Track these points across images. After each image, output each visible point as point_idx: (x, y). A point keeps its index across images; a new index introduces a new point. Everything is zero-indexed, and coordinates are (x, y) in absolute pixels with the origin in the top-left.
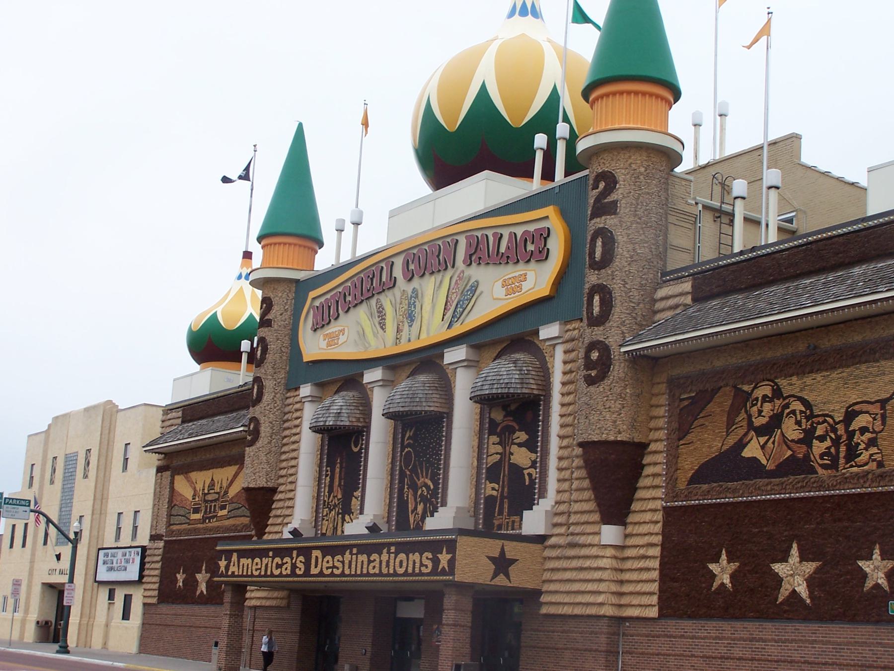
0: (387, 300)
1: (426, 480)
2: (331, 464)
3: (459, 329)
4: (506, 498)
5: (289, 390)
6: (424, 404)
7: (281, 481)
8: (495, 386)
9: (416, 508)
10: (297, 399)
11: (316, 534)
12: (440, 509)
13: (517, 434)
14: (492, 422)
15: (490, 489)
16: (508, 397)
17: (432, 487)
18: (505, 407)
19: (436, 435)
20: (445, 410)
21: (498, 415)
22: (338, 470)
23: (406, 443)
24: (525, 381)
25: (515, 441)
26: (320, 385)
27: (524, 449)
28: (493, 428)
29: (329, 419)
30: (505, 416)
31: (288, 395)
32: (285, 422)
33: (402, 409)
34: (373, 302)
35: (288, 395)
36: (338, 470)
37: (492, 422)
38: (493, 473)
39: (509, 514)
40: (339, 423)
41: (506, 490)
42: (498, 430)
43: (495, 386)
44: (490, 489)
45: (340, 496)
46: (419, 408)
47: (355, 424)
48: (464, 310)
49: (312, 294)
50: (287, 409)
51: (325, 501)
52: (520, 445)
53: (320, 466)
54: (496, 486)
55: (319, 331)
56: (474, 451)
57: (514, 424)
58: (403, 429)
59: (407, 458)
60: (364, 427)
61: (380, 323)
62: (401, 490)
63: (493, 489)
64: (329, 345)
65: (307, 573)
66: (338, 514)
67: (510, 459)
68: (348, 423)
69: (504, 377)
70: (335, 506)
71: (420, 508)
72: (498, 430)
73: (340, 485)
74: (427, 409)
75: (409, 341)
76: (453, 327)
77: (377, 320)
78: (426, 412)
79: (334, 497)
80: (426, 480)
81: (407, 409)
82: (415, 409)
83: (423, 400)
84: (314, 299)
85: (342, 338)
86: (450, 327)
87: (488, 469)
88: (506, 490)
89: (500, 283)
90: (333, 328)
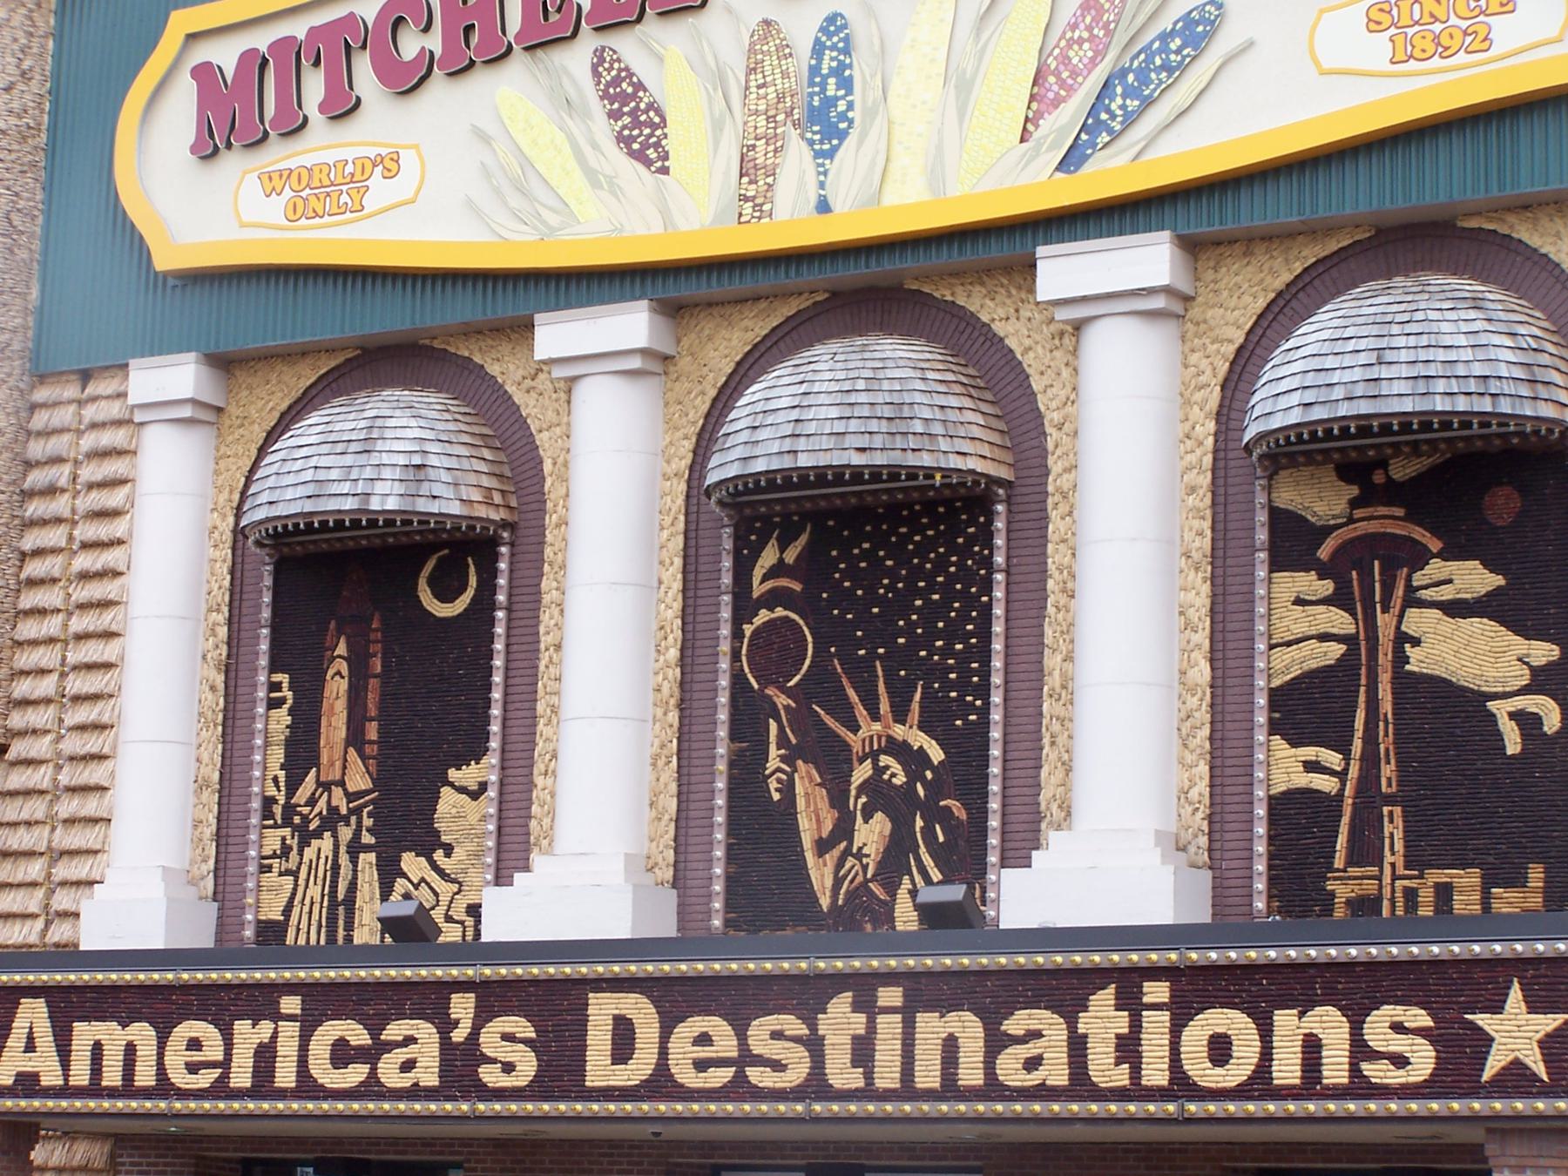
1: (899, 731)
2: (298, 656)
3: (1112, 174)
4: (1390, 800)
5: (42, 378)
6: (944, 444)
7: (17, 720)
8: (1441, 386)
9: (844, 829)
10: (114, 410)
11: (225, 926)
12: (1053, 837)
13: (1436, 568)
14: (1281, 521)
15: (1285, 766)
16: (1446, 425)
17: (936, 754)
18: (1349, 471)
19: (941, 565)
20: (1003, 473)
21: (1322, 500)
22: (337, 688)
23: (758, 589)
24: (1541, 374)
25: (1425, 594)
26: (225, 364)
27: (1480, 628)
28: (1293, 542)
29: (379, 487)
30: (1354, 504)
31: (41, 395)
32: (28, 495)
33: (858, 460)
34: (576, 59)
35: (41, 395)
36: (337, 688)
37: (1281, 521)
38: (1308, 709)
39: (1416, 860)
40: (423, 506)
41: (1388, 771)
42: (1324, 553)
43: (1441, 386)
44: (1285, 766)
45: (359, 780)
46: (926, 460)
47: (482, 512)
48: (1148, 103)
50: (36, 449)
51: (269, 802)
52: (1456, 609)
53: (233, 669)
54: (1333, 759)
55: (233, 164)
56: (1188, 626)
57: (1419, 534)
58: (739, 540)
59: (772, 653)
60: (505, 524)
61: (623, 140)
62: (747, 769)
63: (1312, 767)
64: (295, 212)
65: (263, 1083)
66: (355, 849)
67: (1401, 659)
68: (455, 509)
69: (1467, 355)
70: (332, 820)
71: (872, 834)
72: (1324, 553)
73: (355, 738)
74: (955, 462)
75: (824, 207)
76: (1088, 168)
77: (603, 129)
78: (947, 472)
79: (326, 786)
80: (899, 731)
81: (879, 459)
82: (912, 460)
83: (938, 429)
84: (192, 37)
85: (380, 191)
86: (1071, 160)
87: (1273, 693)
88: (1388, 771)
89: (1357, 14)
90: (323, 145)
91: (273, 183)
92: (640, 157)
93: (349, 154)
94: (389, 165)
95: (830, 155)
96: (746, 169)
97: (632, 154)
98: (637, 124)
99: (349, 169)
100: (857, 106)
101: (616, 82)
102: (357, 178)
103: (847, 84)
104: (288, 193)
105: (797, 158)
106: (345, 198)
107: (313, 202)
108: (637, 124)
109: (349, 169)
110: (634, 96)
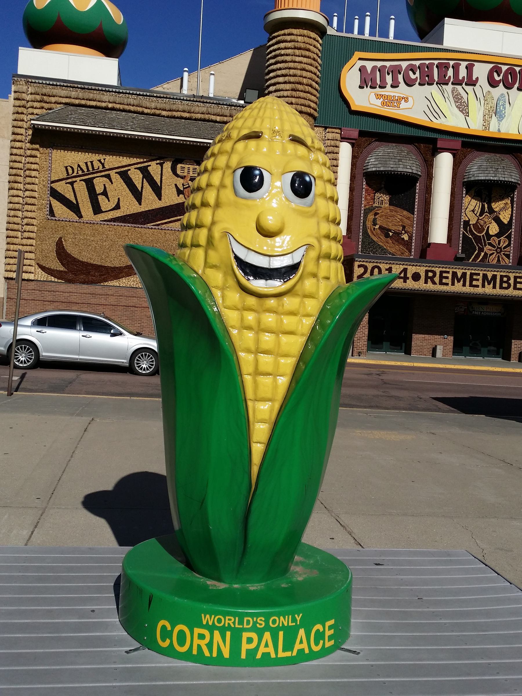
0: (468, 93)
49: (358, 54)
64: (383, 104)
85: (403, 104)
90: (389, 91)
91: (378, 96)
92: (461, 111)
93: (397, 95)
94: (406, 100)
95: (501, 121)
96: (484, 120)
97: (460, 111)
98: (461, 105)
99: (397, 98)
100: (506, 113)
101: (457, 95)
102: (399, 100)
103: (505, 108)
104: (382, 100)
105: (494, 119)
106: (395, 104)
107: (388, 103)
108: (461, 105)
109: (397, 98)
110: (461, 99)
